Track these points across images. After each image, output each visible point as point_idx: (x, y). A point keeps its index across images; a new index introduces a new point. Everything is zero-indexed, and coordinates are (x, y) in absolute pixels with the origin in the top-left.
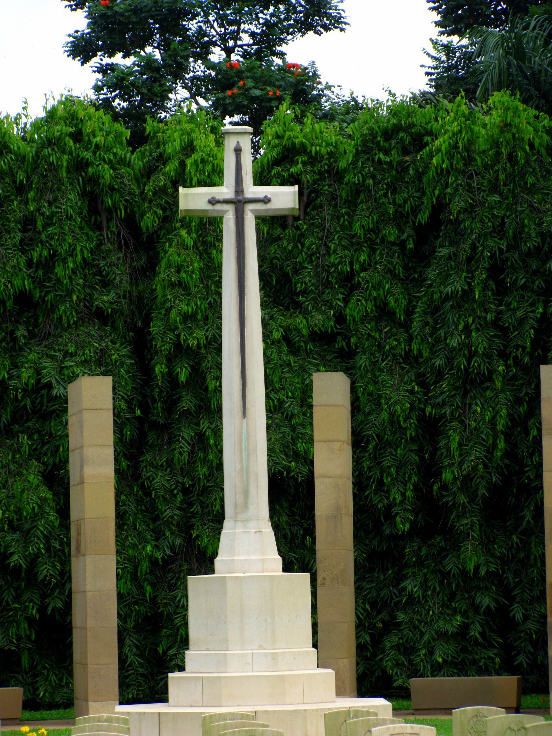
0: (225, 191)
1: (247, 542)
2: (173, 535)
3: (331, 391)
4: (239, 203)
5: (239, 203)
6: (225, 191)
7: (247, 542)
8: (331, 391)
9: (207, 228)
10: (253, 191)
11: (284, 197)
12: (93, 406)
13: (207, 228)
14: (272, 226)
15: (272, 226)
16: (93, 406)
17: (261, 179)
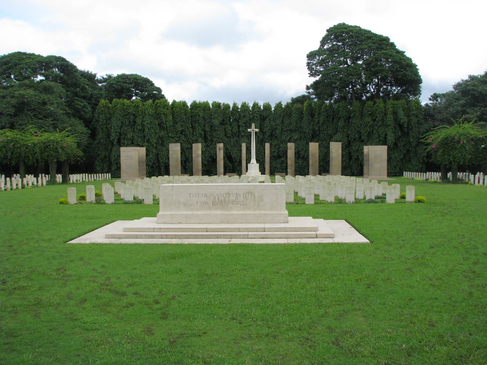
0: (252, 129)
1: (253, 160)
2: (248, 160)
3: (267, 145)
4: (253, 130)
5: (253, 130)
6: (252, 129)
7: (253, 160)
8: (267, 145)
9: (250, 133)
10: (254, 129)
11: (257, 130)
12: (244, 146)
13: (250, 133)
14: (256, 133)
15: (256, 133)
16: (244, 146)
17: (255, 128)
